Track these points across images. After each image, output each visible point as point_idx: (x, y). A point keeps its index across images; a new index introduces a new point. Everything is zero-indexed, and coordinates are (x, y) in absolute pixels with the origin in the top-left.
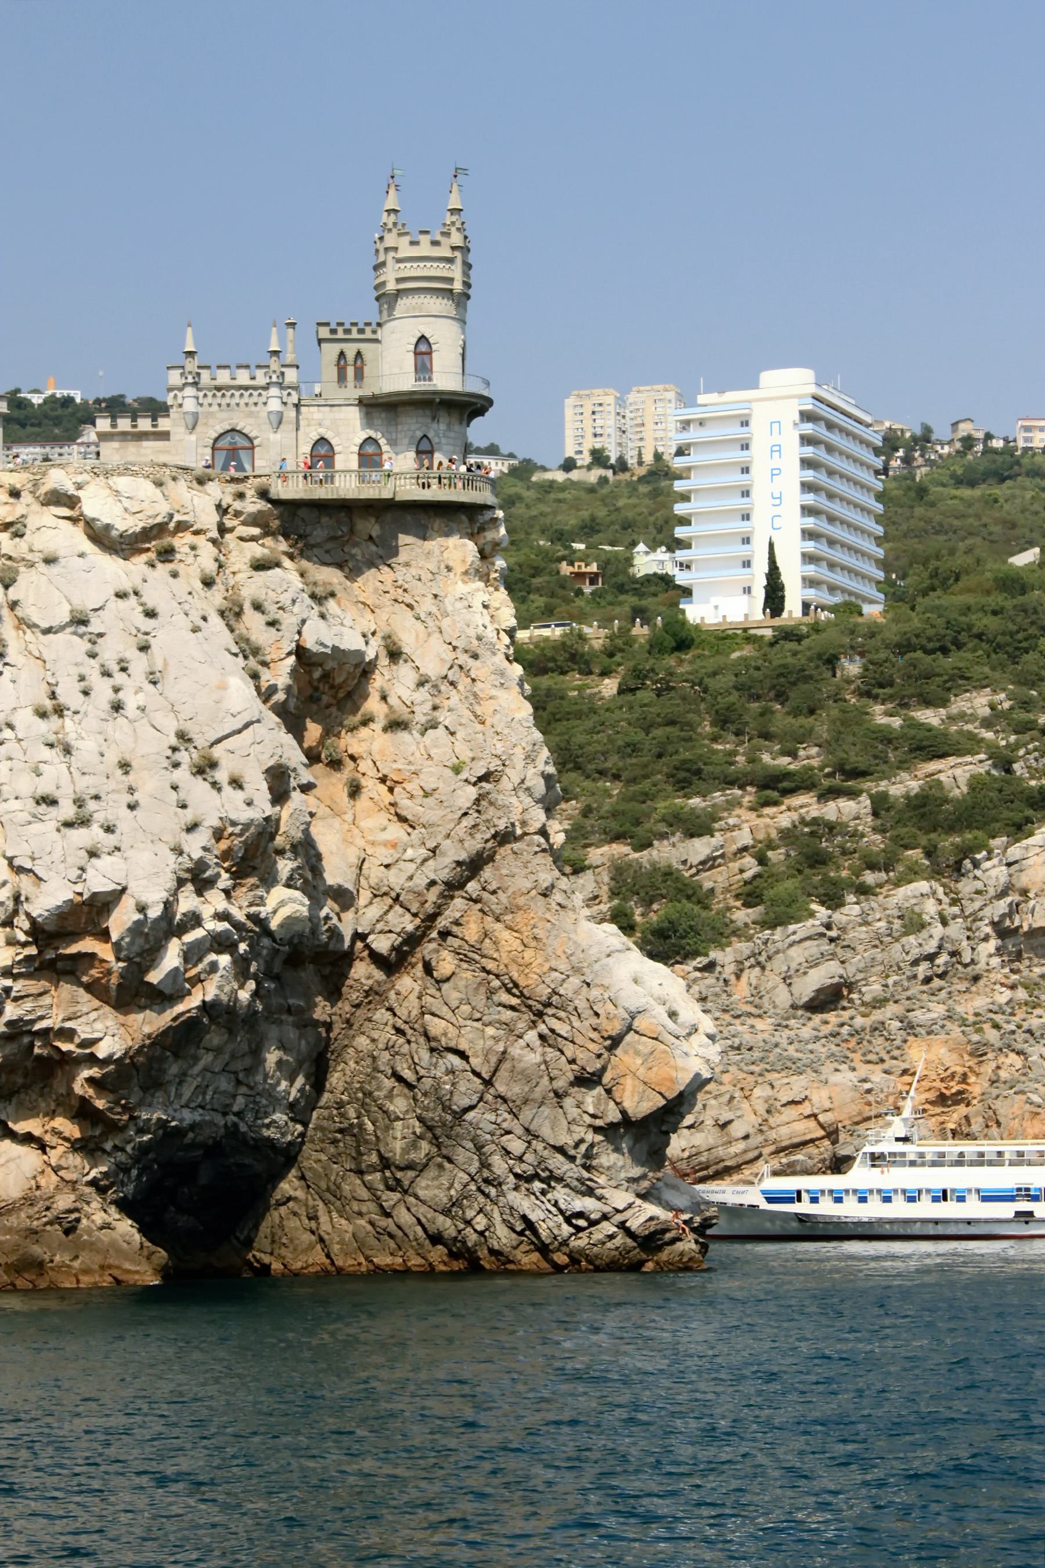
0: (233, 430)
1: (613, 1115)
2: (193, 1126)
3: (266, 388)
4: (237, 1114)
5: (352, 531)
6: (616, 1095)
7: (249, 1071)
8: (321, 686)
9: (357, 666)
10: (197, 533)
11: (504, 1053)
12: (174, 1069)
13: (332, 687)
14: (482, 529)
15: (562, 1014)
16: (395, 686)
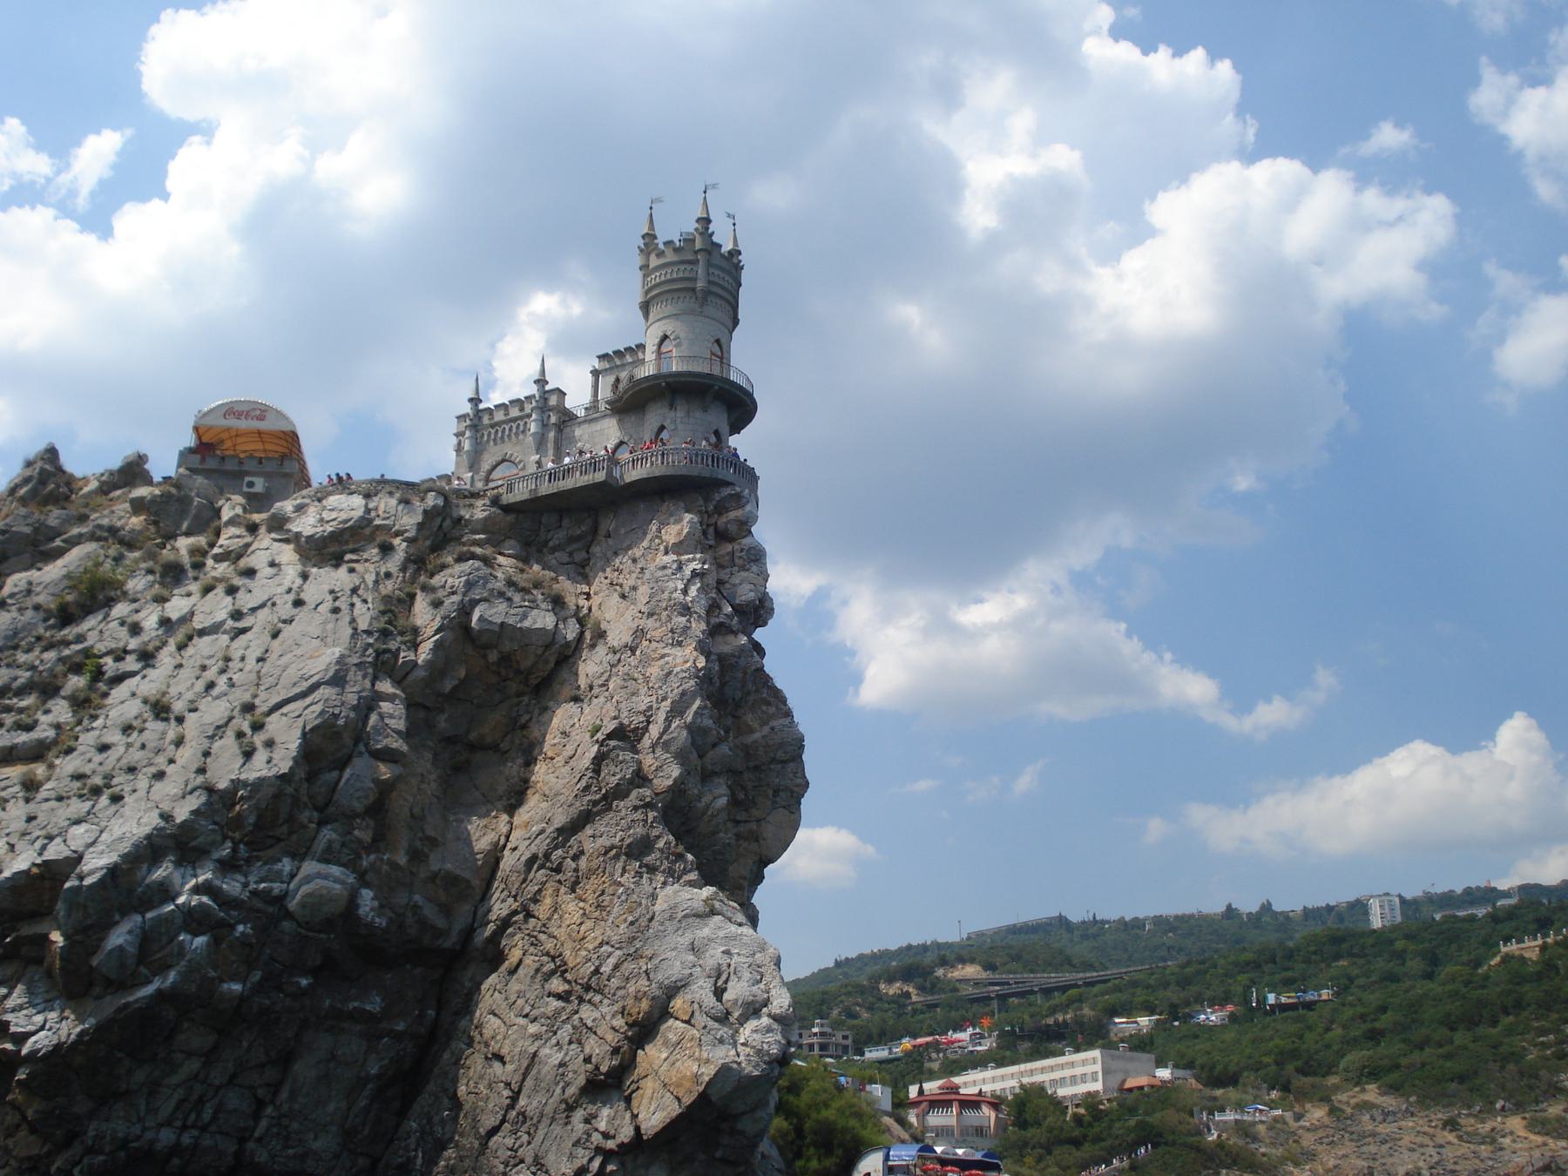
0: (503, 461)
1: (626, 1134)
2: (175, 1149)
3: (529, 416)
4: (259, 1140)
5: (595, 530)
6: (634, 1103)
7: (275, 1087)
8: (503, 672)
9: (547, 647)
11: (535, 1054)
12: (140, 1076)
13: (518, 672)
14: (721, 509)
15: (598, 998)
16: (590, 666)
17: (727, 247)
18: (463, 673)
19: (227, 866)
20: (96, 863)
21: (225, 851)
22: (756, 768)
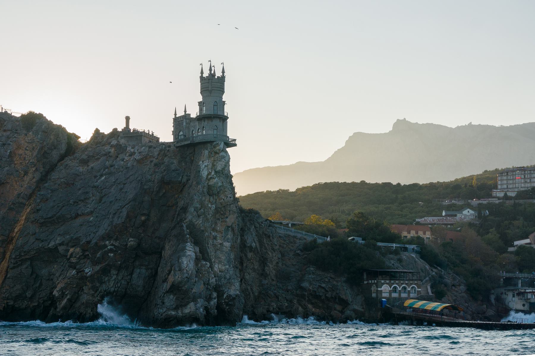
2: (114, 291)
10: (154, 157)
12: (106, 279)
14: (215, 147)
17: (219, 74)
18: (164, 191)
19: (116, 240)
20: (94, 241)
21: (115, 238)
22: (224, 207)
